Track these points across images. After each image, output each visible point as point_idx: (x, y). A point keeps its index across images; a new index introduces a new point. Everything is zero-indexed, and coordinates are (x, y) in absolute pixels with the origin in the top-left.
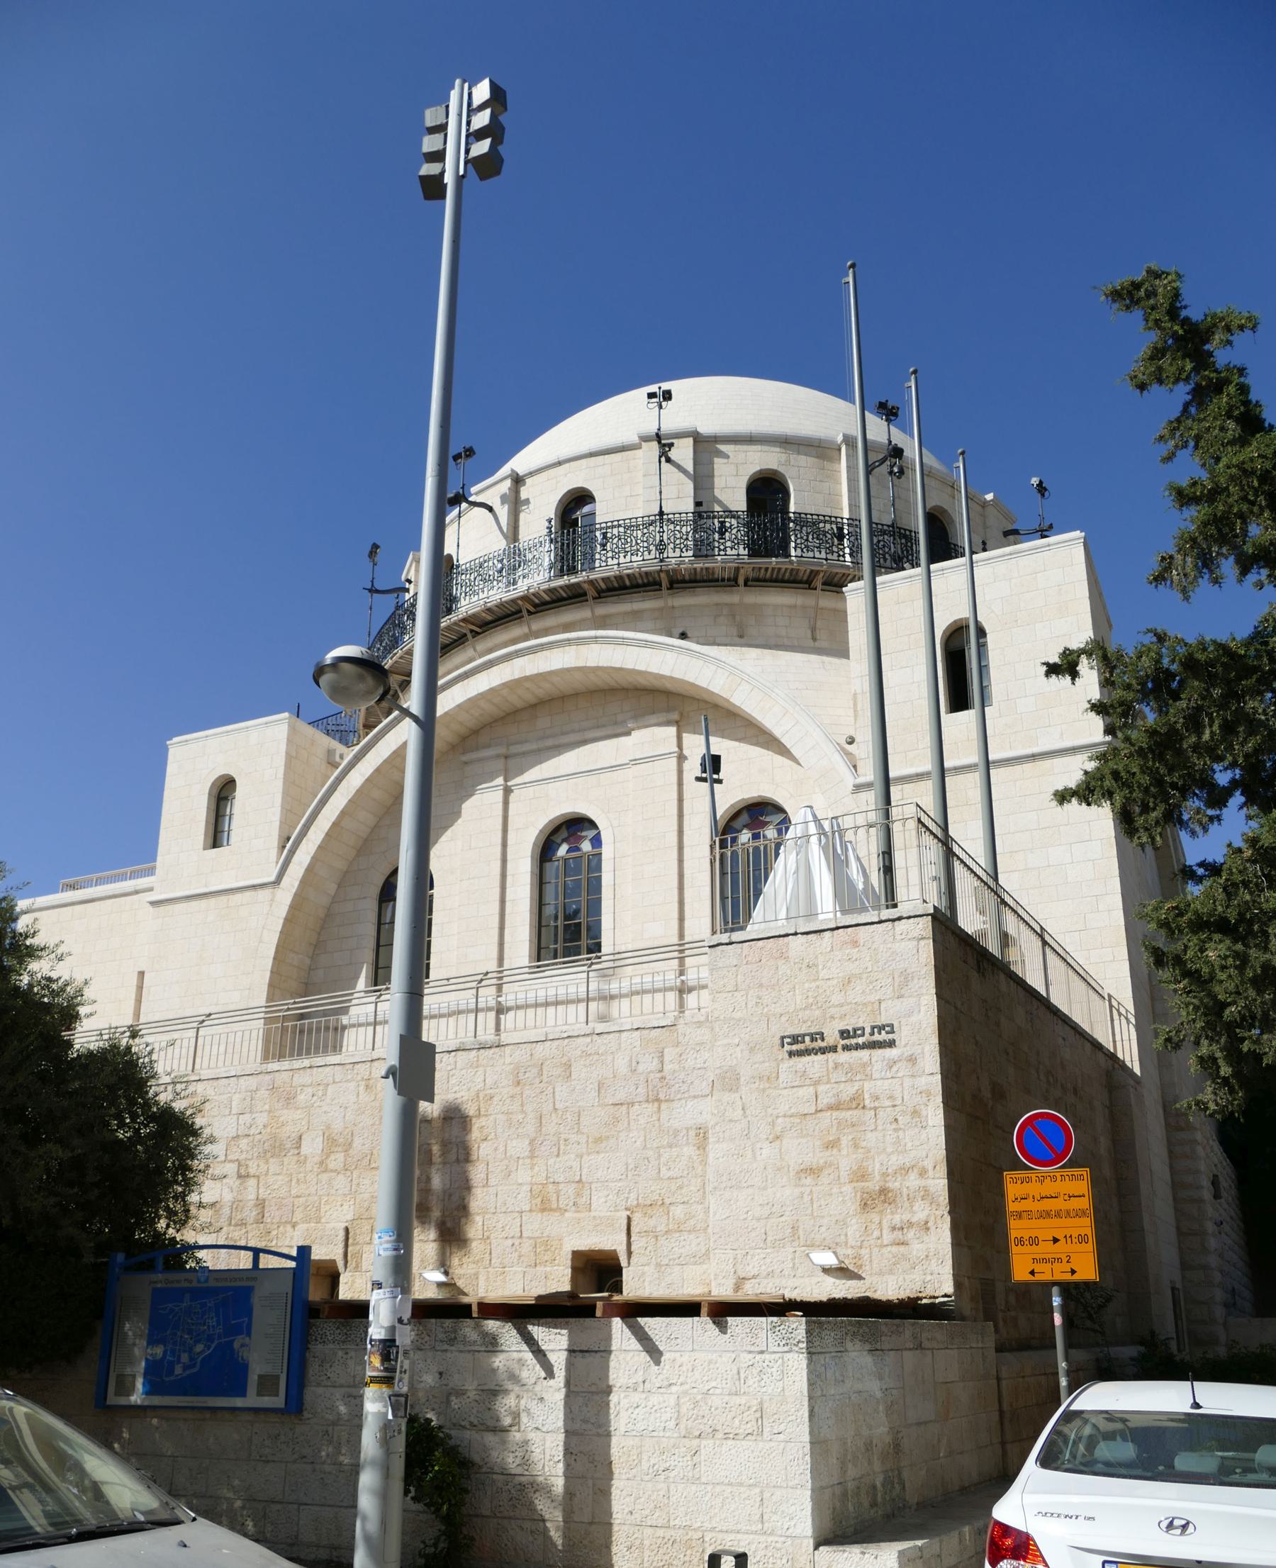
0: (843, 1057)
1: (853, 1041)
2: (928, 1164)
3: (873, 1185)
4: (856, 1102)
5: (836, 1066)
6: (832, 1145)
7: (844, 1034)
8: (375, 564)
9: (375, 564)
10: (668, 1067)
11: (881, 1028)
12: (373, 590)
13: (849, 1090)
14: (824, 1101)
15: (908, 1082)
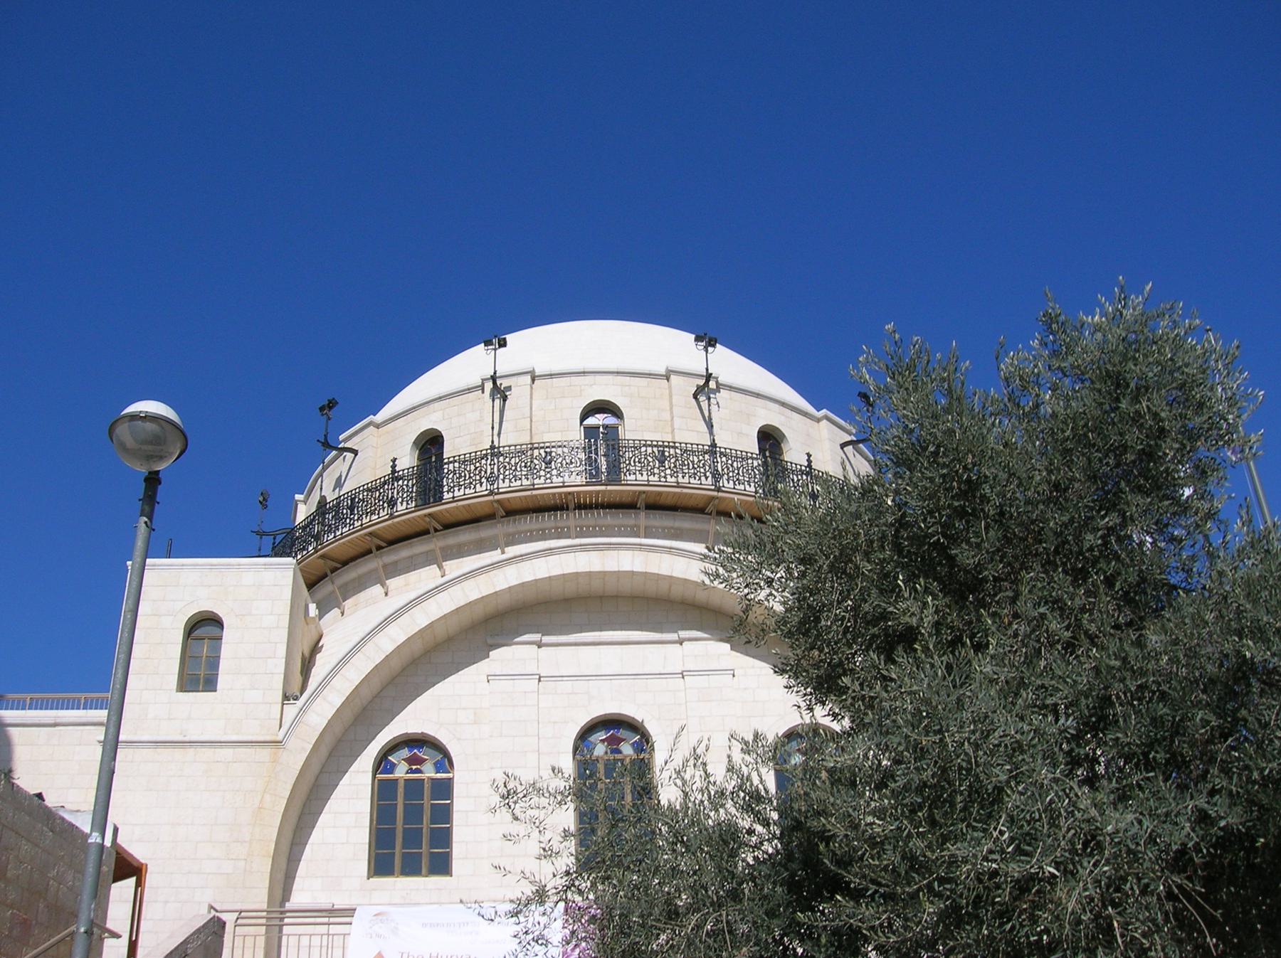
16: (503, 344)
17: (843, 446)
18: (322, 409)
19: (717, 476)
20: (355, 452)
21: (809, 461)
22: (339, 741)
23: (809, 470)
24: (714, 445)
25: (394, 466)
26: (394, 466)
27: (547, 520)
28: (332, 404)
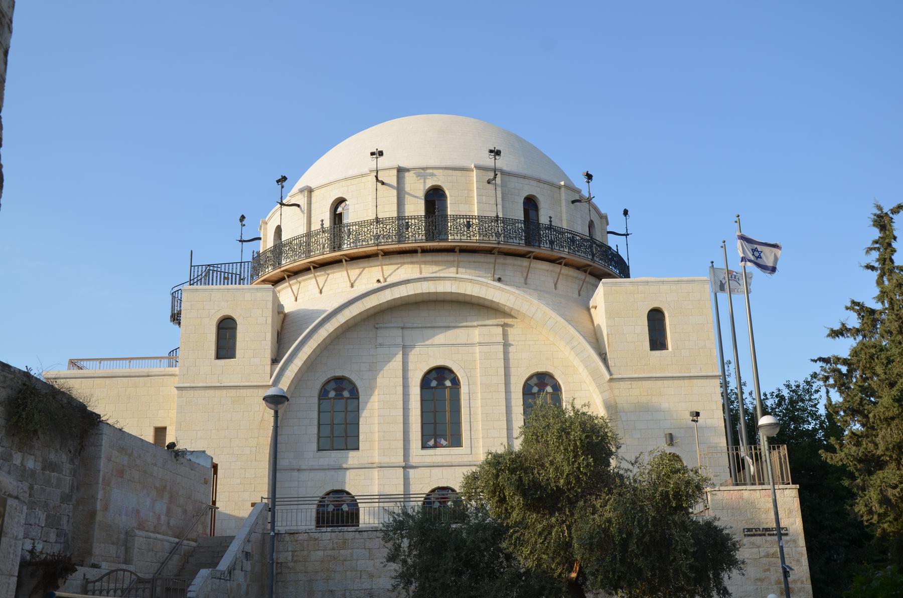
0: (769, 538)
2: (804, 579)
6: (769, 570)
8: (282, 187)
9: (282, 187)
12: (282, 204)
14: (762, 554)
15: (794, 549)
16: (381, 153)
17: (573, 202)
18: (278, 181)
19: (498, 235)
20: (298, 206)
21: (551, 221)
22: (300, 380)
23: (550, 227)
24: (497, 217)
25: (322, 225)
26: (322, 225)
27: (407, 258)
28: (284, 179)
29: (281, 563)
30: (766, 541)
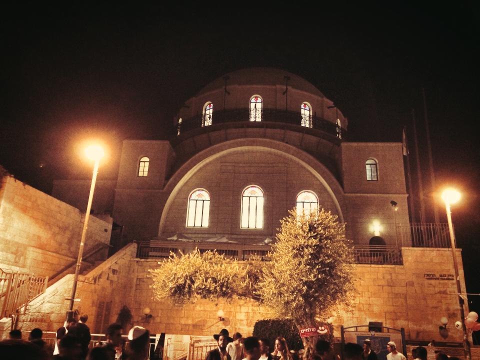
0: (442, 281)
1: (443, 278)
3: (451, 312)
4: (445, 292)
5: (440, 283)
7: (441, 276)
10: (393, 278)
11: (450, 275)
13: (442, 289)
24: (287, 110)
29: (140, 279)
30: (440, 283)
